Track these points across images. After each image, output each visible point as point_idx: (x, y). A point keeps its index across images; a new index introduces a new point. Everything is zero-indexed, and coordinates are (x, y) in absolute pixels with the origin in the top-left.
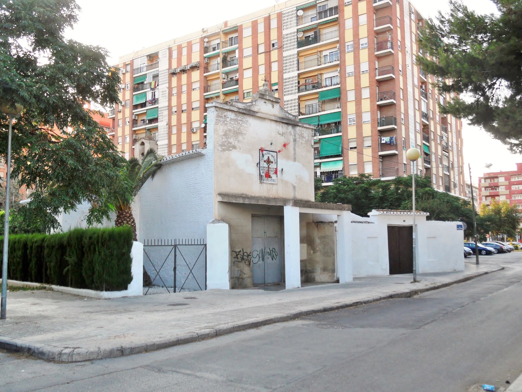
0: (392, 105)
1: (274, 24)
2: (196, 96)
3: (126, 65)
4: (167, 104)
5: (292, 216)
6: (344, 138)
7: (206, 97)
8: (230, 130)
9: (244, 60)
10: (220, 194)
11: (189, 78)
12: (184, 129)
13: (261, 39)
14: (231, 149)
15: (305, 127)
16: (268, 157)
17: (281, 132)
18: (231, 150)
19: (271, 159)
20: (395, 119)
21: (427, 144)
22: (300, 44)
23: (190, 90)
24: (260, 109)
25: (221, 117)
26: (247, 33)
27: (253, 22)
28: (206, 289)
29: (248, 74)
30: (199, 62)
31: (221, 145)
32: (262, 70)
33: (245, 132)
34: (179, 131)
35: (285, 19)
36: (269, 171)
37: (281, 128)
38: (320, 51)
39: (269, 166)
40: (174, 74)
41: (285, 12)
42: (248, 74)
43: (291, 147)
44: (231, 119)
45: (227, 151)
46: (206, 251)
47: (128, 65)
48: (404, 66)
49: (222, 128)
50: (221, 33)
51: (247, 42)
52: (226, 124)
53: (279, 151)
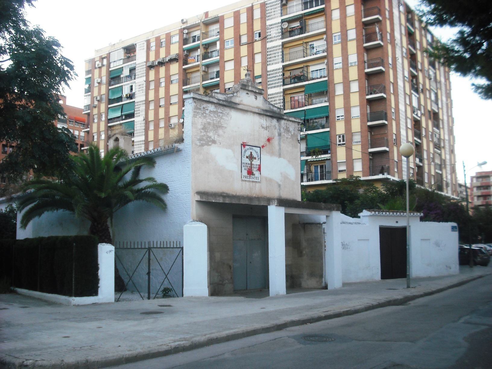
0: (382, 99)
1: (257, 14)
2: (174, 89)
3: (102, 59)
4: (144, 98)
5: (276, 218)
6: (333, 134)
7: (185, 90)
8: (209, 123)
9: (226, 52)
10: (198, 193)
11: (167, 71)
12: (162, 124)
13: (244, 29)
14: (210, 143)
15: (291, 121)
16: (251, 153)
17: (265, 126)
18: (210, 145)
19: (254, 155)
20: (386, 114)
21: (419, 141)
22: (284, 33)
23: (169, 82)
24: (241, 101)
25: (200, 109)
26: (229, 23)
27: (235, 13)
28: (183, 295)
29: (230, 66)
30: (177, 55)
31: (200, 140)
32: (245, 62)
33: (225, 125)
34: (157, 127)
35: (269, 9)
36: (251, 167)
37: (264, 121)
38: (306, 43)
39: (251, 162)
40: (151, 67)
41: (268, 2)
42: (230, 66)
43: (275, 142)
44: (210, 111)
45: (206, 146)
46: (183, 254)
47: (104, 58)
48: (394, 59)
49: (200, 120)
50: (202, 25)
51: (229, 34)
52: (205, 117)
53: (263, 146)
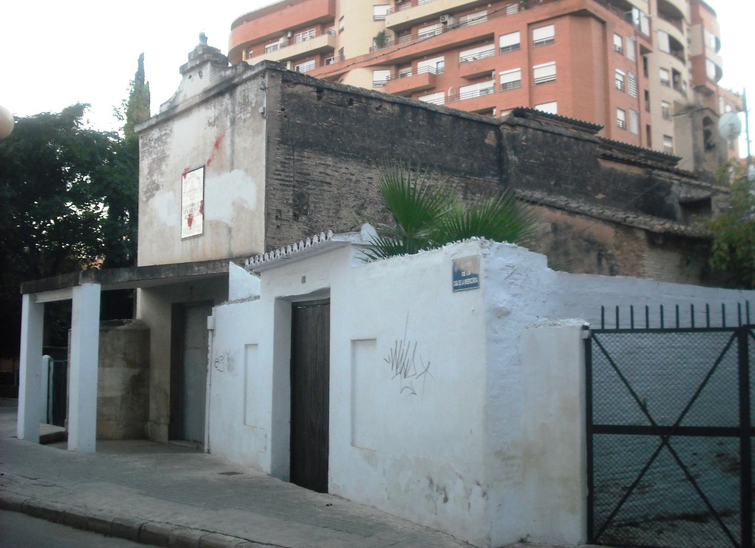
24: (185, 96)
53: (209, 161)
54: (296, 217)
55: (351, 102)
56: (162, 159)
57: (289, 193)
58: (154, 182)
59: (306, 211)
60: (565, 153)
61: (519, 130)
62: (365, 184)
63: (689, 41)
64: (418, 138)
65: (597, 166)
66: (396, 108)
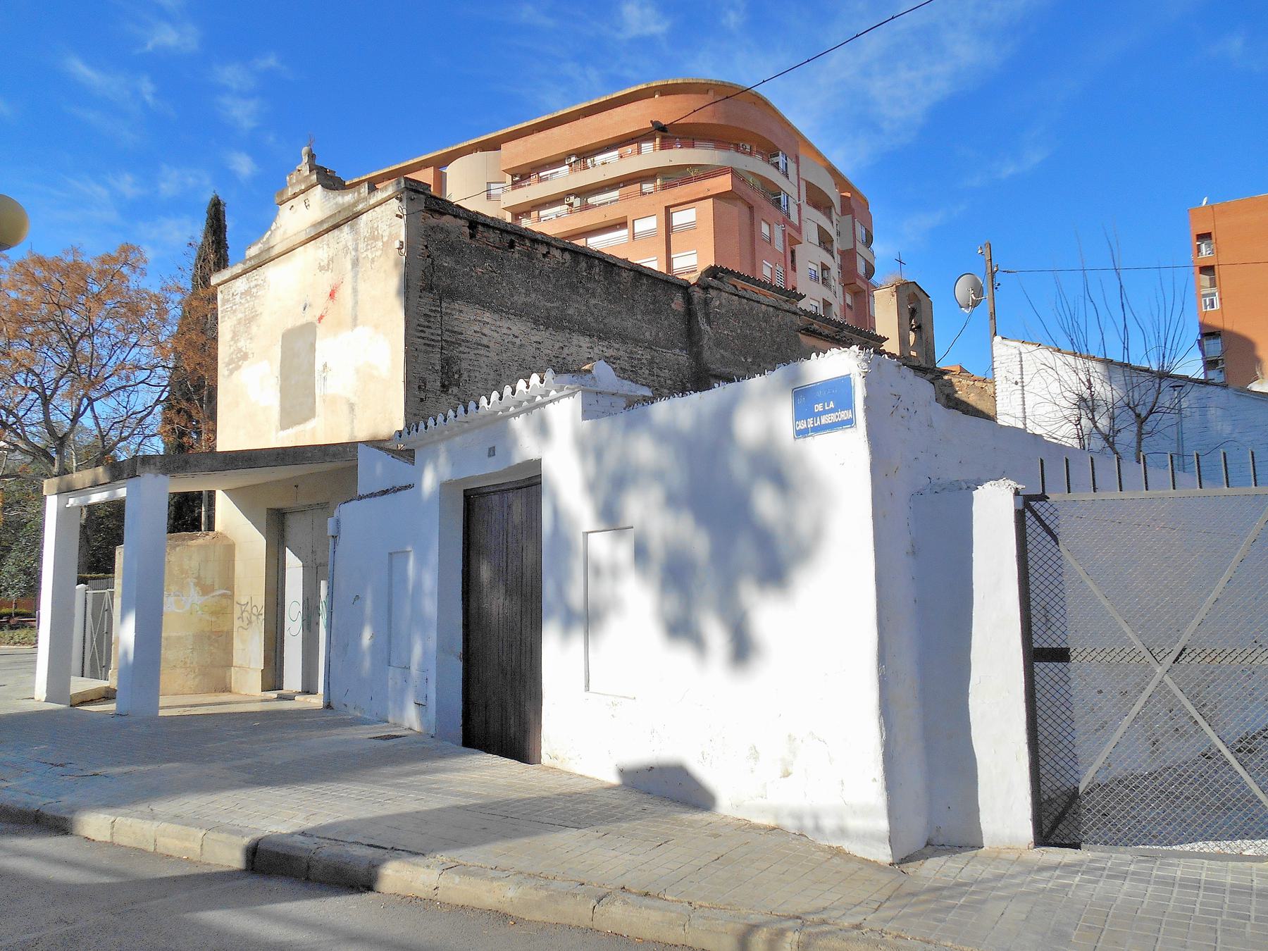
24: (285, 232)
54: (445, 388)
55: (512, 245)
56: (250, 319)
57: (436, 358)
58: (240, 350)
59: (458, 380)
60: (764, 325)
61: (713, 293)
62: (531, 350)
63: (838, 234)
64: (593, 295)
65: (798, 342)
66: (567, 256)
